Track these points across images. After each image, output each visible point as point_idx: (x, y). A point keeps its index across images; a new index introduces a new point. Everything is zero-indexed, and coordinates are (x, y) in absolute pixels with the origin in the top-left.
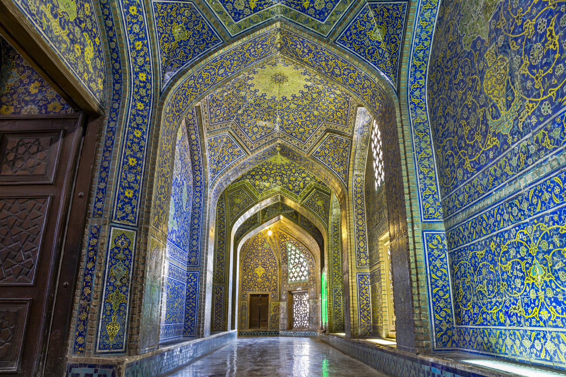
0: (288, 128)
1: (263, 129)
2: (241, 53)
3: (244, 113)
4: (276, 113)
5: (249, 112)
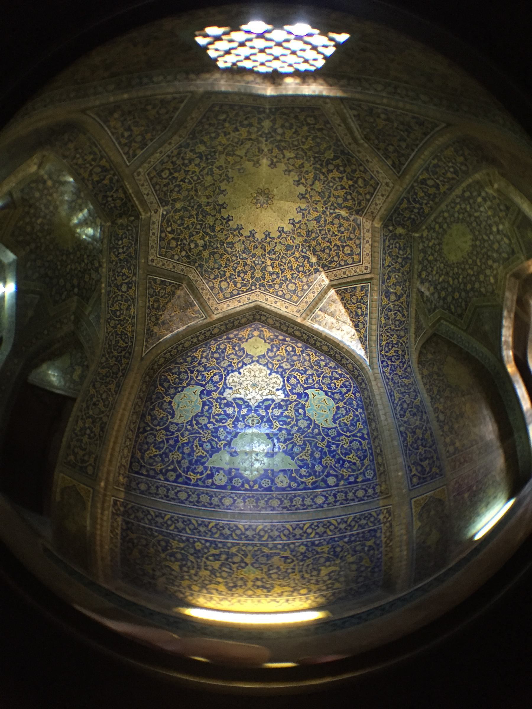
0: (359, 204)
1: (351, 239)
2: (117, 263)
3: (318, 256)
4: (331, 214)
5: (318, 248)
